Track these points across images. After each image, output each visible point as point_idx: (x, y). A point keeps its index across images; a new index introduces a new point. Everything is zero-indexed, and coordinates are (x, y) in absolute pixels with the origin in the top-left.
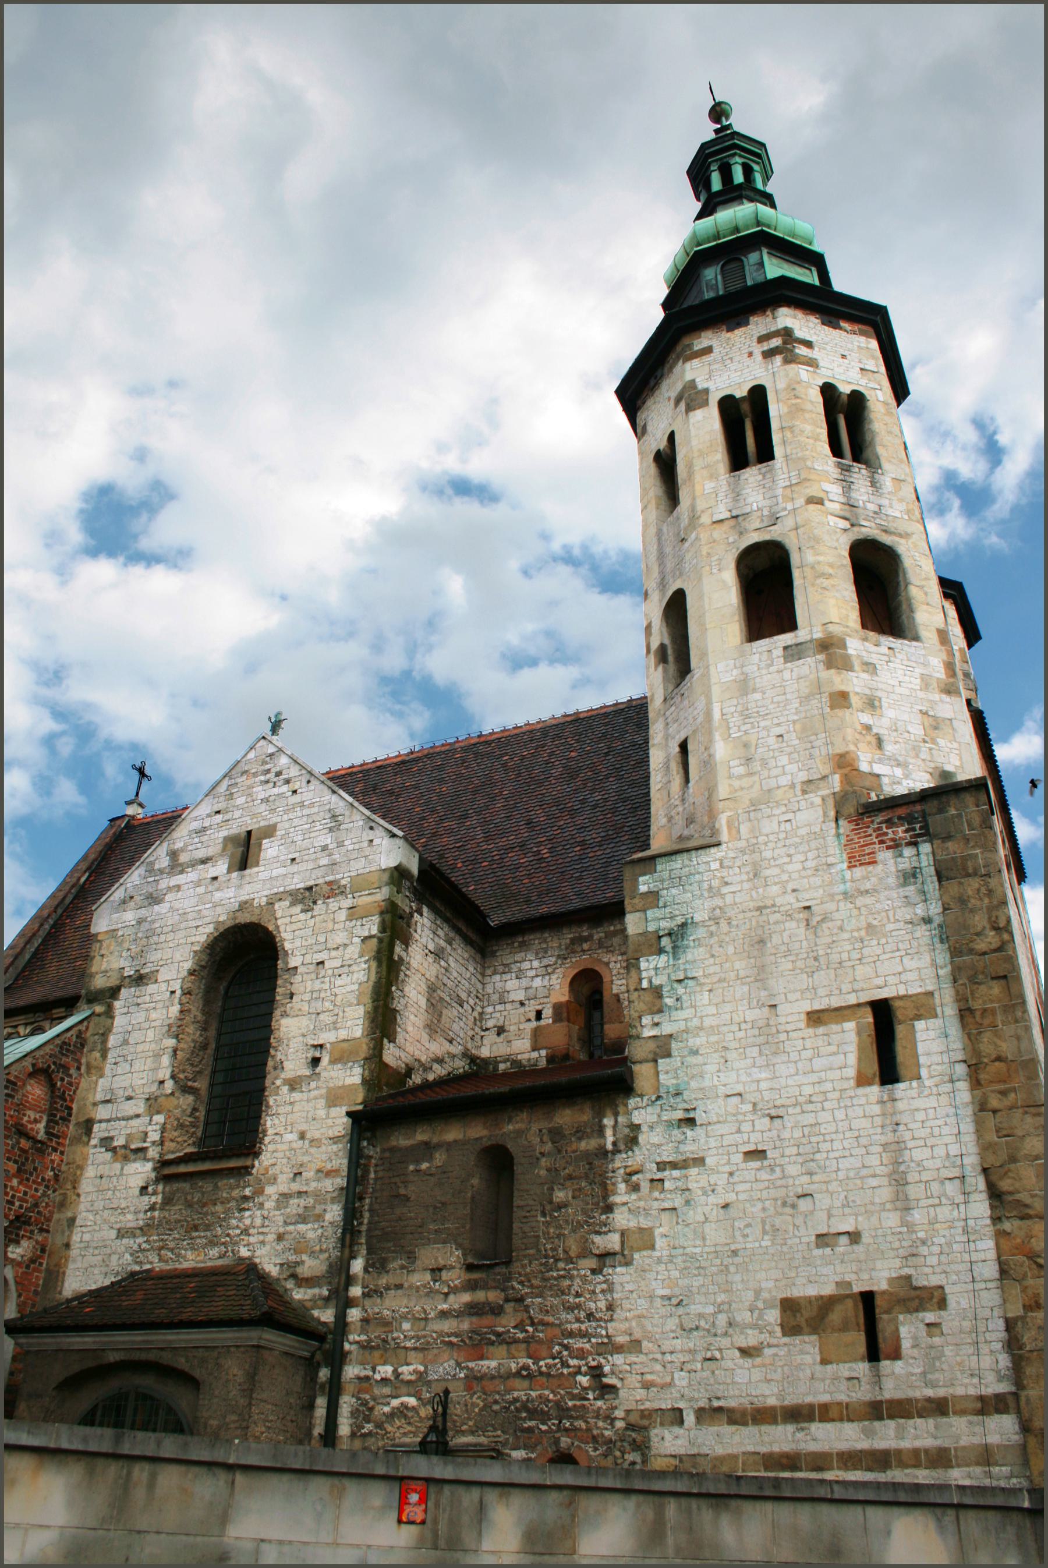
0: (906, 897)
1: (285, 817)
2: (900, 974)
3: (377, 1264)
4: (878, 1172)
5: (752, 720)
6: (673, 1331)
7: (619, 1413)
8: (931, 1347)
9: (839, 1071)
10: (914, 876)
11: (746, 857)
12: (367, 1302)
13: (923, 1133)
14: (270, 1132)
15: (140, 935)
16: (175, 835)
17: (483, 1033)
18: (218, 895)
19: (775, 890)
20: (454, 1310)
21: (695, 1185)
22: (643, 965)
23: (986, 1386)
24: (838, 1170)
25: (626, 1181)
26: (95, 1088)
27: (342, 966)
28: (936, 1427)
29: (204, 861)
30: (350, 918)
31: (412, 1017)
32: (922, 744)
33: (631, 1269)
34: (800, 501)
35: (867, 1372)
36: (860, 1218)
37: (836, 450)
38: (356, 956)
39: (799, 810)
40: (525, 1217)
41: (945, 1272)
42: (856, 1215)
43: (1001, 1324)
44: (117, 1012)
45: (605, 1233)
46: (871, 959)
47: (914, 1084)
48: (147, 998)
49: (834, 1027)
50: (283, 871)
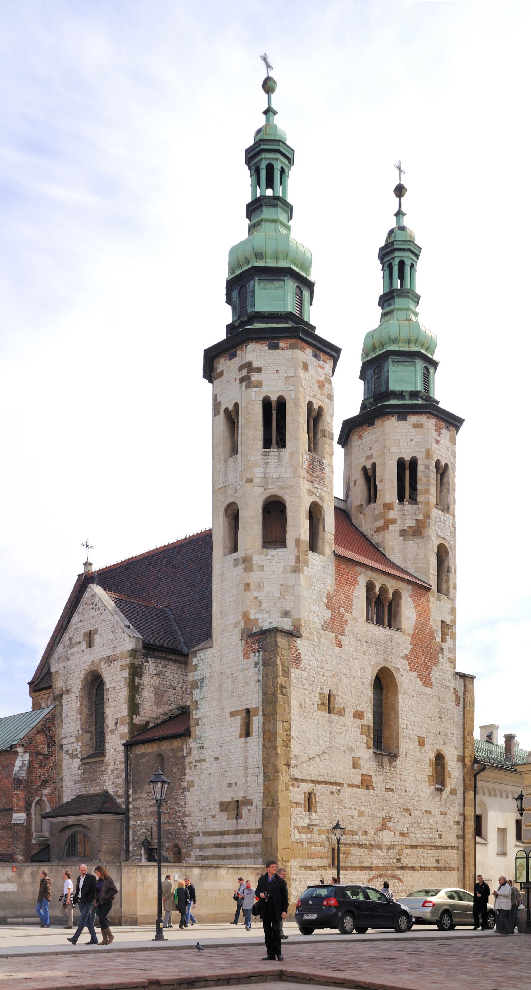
1: (100, 625)
3: (135, 792)
7: (187, 833)
12: (134, 803)
14: (107, 748)
18: (85, 658)
22: (193, 692)
29: (79, 643)
31: (147, 703)
43: (261, 810)
49: (236, 718)
50: (100, 649)
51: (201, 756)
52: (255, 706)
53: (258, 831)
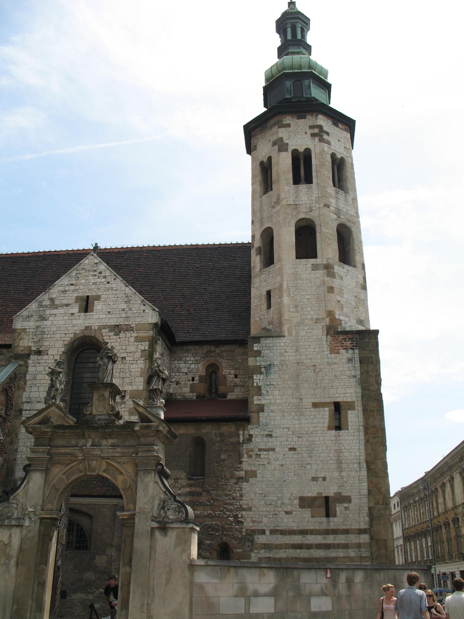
0: (349, 367)
1: (105, 293)
2: (344, 394)
4: (333, 459)
5: (298, 291)
6: (262, 505)
7: (244, 530)
8: (346, 514)
9: (322, 424)
10: (352, 360)
11: (294, 343)
13: (348, 447)
15: (38, 333)
16: (51, 291)
17: (170, 383)
18: (75, 322)
19: (304, 357)
20: (184, 493)
21: (271, 457)
22: (255, 377)
23: (361, 526)
24: (320, 457)
25: (246, 454)
26: (22, 397)
27: (133, 360)
28: (345, 537)
29: (67, 305)
30: (136, 341)
32: (355, 309)
33: (248, 484)
34: (322, 205)
35: (325, 520)
36: (326, 473)
37: (334, 185)
38: (139, 357)
39: (314, 329)
40: (210, 463)
41: (352, 492)
42: (325, 472)
43: (367, 508)
44: (30, 365)
45: (240, 471)
46: (335, 387)
47: (346, 431)
48: (44, 361)
49: (322, 409)
51: (267, 444)
52: (349, 400)
53: (361, 532)
